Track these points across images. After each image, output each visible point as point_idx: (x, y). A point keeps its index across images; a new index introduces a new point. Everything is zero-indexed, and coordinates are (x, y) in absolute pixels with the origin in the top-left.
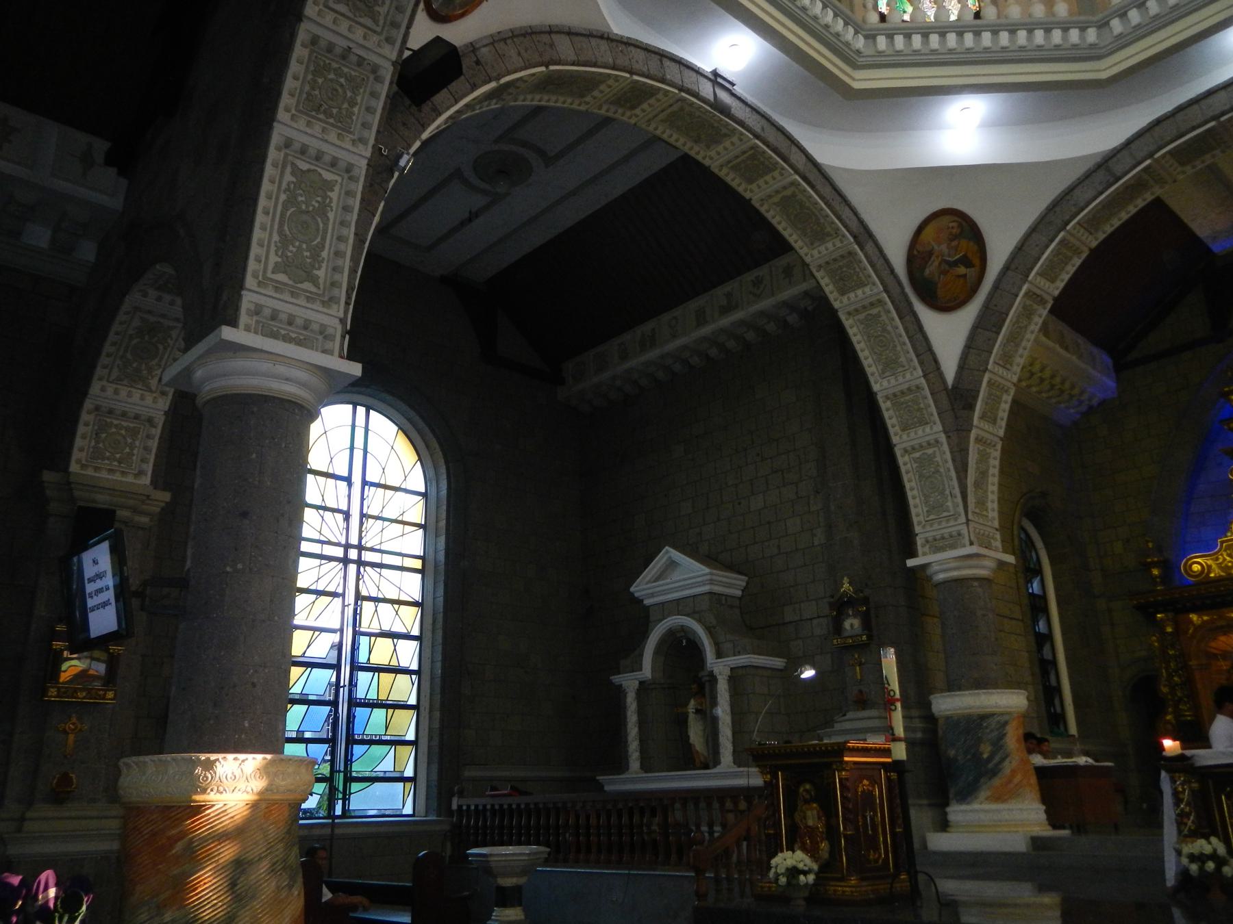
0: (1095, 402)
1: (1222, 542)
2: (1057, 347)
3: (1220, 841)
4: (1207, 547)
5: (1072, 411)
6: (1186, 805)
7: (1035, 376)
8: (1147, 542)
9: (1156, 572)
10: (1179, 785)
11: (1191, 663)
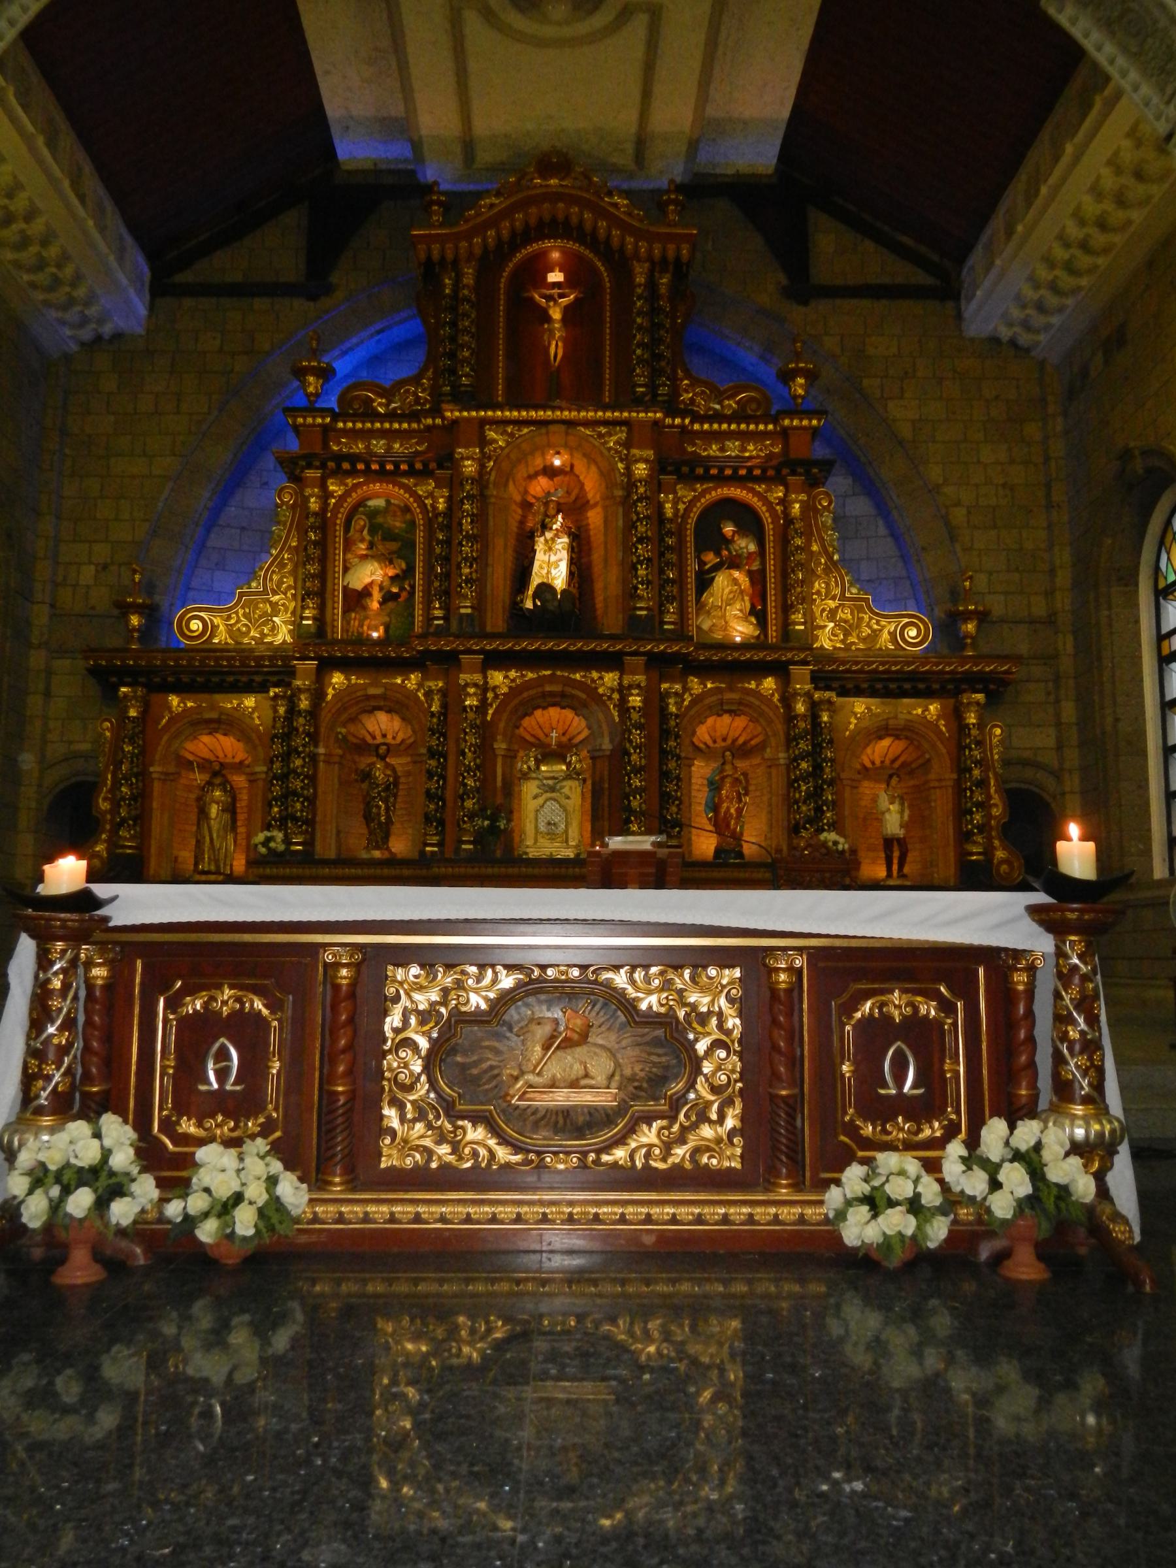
0: (107, 329)
1: (242, 595)
2: (66, 184)
3: (126, 1122)
4: (218, 598)
5: (68, 332)
6: (61, 1029)
7: (14, 227)
8: (135, 572)
9: (135, 620)
10: (56, 974)
11: (152, 769)
